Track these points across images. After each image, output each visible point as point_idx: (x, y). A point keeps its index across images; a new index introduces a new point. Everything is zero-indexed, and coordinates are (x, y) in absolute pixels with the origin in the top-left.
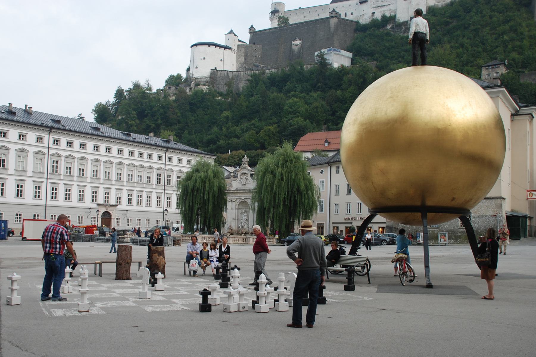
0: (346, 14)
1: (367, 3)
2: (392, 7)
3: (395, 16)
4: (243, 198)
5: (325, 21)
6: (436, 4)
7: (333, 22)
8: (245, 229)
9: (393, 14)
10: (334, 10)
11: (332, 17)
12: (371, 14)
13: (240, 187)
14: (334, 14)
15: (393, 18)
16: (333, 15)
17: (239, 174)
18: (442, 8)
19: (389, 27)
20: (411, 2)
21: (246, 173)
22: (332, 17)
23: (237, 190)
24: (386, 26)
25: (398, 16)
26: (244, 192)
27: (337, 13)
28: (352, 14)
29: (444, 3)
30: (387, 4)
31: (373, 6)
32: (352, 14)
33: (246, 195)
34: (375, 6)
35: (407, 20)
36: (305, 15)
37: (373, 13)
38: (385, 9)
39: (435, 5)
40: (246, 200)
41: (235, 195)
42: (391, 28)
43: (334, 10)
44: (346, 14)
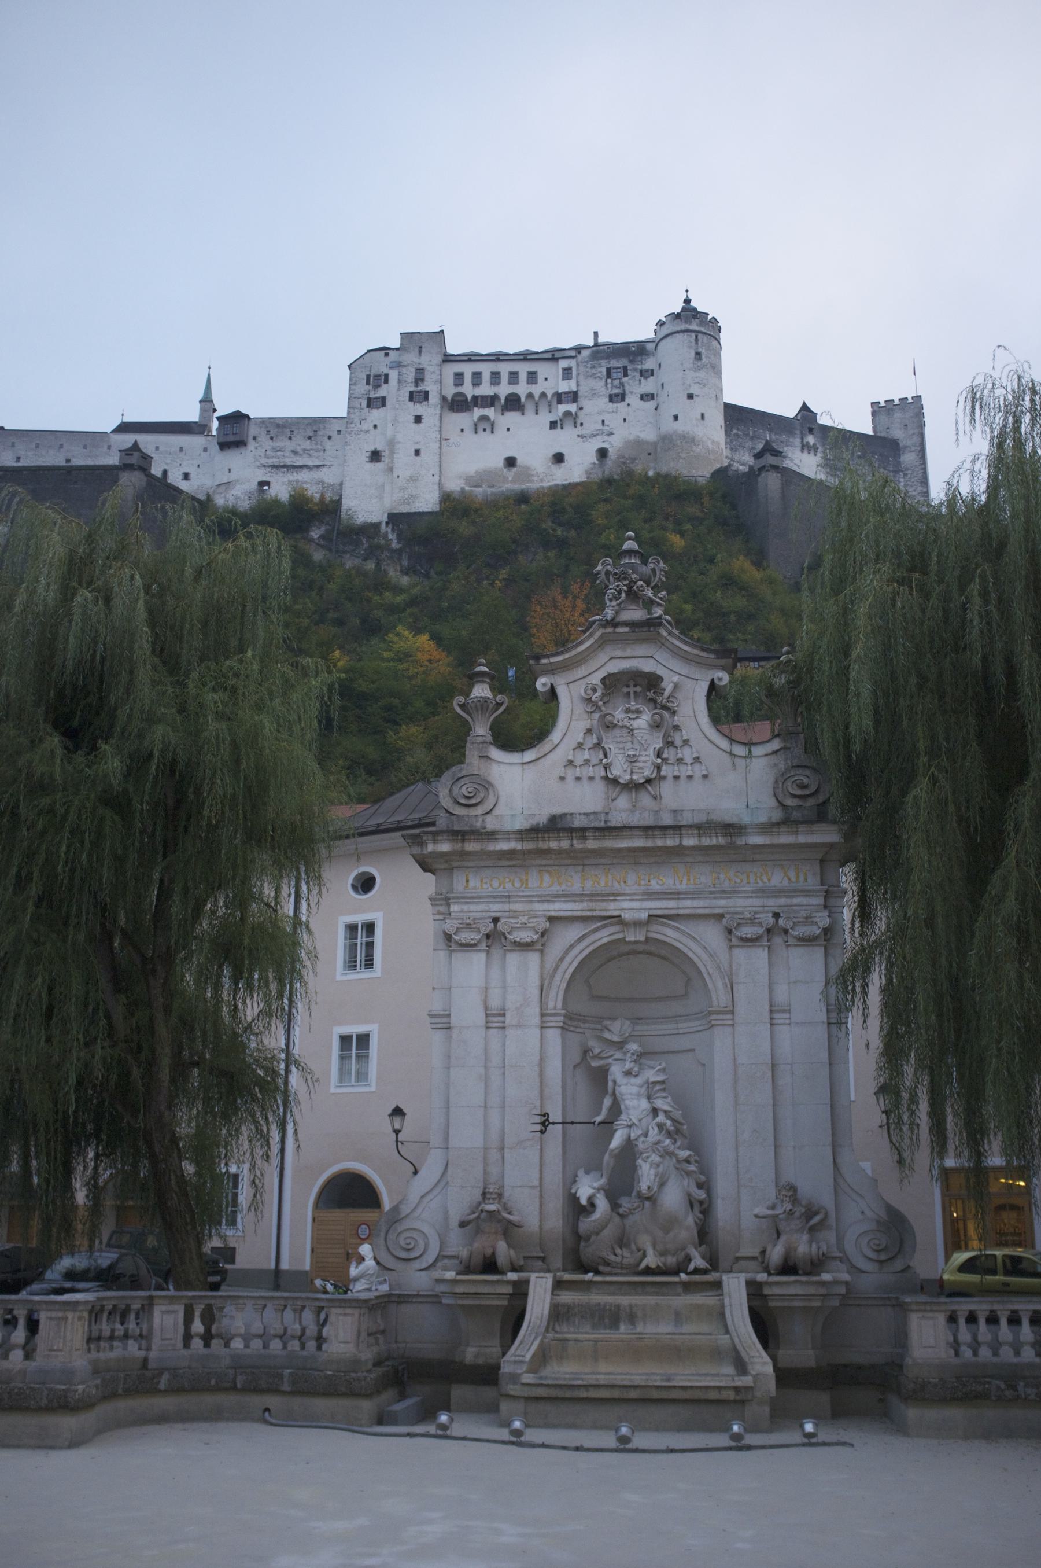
0: (165, 472)
1: (242, 450)
2: (328, 476)
3: (338, 503)
4: (632, 909)
5: (104, 476)
6: (467, 488)
7: (131, 481)
8: (670, 1224)
9: (329, 496)
10: (135, 447)
11: (126, 467)
12: (254, 486)
13: (585, 799)
14: (136, 461)
15: (329, 510)
16: (134, 460)
17: (571, 692)
18: (495, 503)
19: (315, 533)
20: (391, 470)
21: (651, 683)
22: (126, 467)
23: (556, 825)
24: (307, 530)
25: (346, 503)
26: (665, 843)
27: (147, 458)
28: (186, 476)
29: (489, 490)
30: (310, 463)
31: (264, 461)
32: (186, 476)
33: (666, 879)
34: (270, 461)
35: (374, 519)
36: (21, 453)
37: (262, 484)
38: (304, 476)
39: (463, 489)
40: (669, 934)
41: (538, 881)
42: (322, 537)
43: (135, 447)
44: (165, 472)
